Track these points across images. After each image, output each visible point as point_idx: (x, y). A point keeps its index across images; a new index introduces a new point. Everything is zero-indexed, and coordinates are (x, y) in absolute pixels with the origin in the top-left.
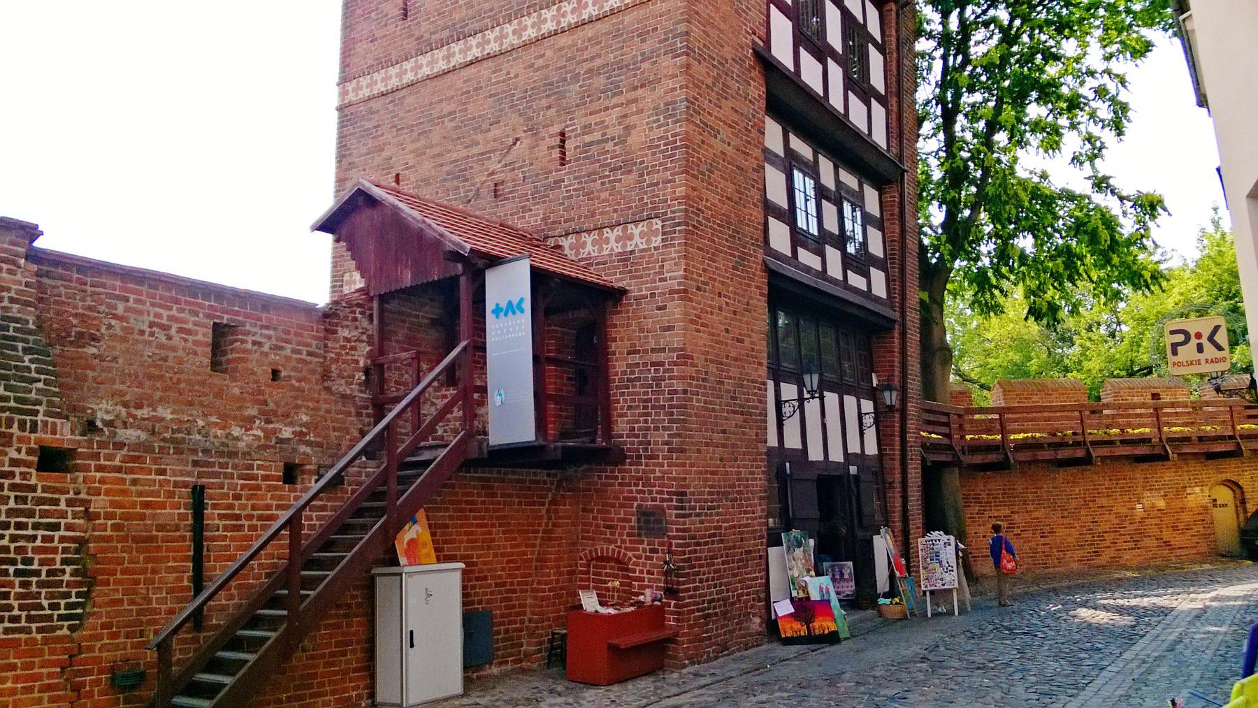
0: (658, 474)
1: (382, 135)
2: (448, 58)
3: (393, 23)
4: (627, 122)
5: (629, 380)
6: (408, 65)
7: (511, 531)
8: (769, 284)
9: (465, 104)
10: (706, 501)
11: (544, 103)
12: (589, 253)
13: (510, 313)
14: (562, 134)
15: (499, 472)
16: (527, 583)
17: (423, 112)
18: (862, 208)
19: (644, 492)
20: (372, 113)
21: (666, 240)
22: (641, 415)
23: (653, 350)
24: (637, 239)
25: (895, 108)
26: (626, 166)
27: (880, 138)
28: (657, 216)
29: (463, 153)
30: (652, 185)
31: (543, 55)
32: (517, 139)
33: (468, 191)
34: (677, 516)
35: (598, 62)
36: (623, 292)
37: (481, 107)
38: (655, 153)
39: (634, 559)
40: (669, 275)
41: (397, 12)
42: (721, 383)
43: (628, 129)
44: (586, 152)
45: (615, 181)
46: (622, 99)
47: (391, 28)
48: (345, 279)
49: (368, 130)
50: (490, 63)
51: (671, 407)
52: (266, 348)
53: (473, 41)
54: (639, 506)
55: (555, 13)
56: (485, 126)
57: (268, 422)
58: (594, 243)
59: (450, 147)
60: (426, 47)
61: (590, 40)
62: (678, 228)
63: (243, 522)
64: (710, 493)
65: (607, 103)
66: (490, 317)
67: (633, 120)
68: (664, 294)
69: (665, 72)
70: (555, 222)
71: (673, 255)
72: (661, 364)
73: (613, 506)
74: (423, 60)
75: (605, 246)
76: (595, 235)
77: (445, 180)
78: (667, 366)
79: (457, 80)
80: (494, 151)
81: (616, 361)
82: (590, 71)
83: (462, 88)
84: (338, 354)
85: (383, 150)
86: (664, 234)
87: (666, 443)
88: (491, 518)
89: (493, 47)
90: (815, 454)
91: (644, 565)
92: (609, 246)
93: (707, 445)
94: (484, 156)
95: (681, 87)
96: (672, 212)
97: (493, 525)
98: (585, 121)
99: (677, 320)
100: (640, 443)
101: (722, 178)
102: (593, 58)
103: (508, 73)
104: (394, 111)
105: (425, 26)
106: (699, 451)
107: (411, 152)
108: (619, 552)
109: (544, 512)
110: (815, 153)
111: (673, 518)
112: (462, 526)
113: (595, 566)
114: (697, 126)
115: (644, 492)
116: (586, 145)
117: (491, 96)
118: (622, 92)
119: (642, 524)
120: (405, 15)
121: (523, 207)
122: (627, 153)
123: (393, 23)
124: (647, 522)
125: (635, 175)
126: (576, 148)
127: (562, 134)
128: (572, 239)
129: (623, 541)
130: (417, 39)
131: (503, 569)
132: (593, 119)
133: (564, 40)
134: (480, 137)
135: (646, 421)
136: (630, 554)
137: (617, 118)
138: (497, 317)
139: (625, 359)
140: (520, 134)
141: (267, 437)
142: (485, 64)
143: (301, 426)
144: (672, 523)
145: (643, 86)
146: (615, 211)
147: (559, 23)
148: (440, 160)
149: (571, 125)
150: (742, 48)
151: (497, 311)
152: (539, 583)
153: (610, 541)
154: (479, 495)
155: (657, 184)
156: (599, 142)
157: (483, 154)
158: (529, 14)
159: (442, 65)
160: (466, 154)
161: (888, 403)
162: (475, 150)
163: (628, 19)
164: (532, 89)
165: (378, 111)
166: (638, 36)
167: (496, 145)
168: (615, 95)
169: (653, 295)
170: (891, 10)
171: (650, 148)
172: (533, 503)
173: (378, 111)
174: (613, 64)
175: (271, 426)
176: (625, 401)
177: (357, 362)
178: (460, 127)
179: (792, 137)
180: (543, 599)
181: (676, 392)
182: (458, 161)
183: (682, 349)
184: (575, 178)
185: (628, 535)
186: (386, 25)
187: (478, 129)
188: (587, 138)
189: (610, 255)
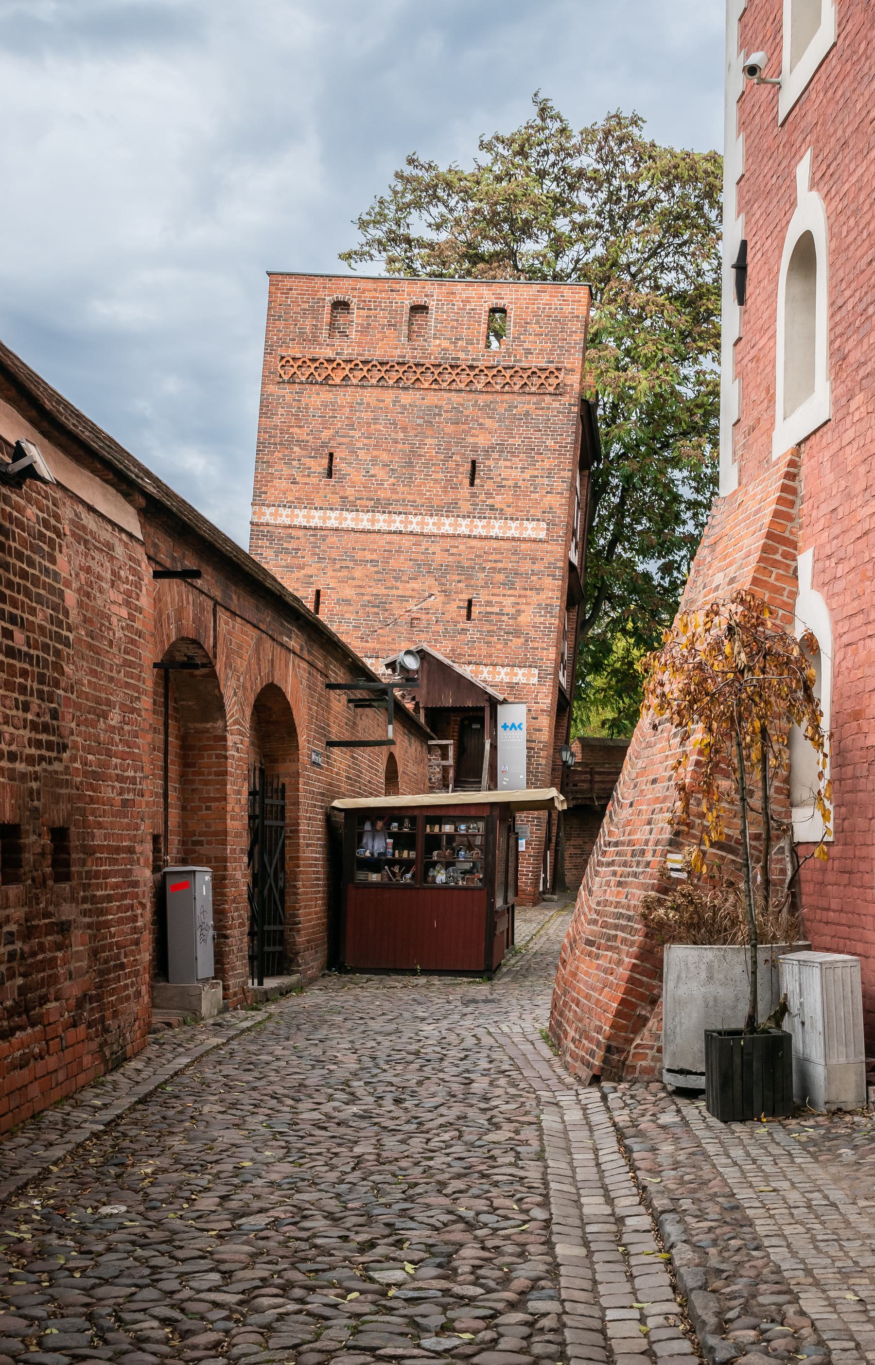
4: (519, 607)
11: (457, 578)
14: (470, 602)
26: (517, 633)
37: (398, 563)
46: (516, 593)
47: (314, 480)
56: (404, 578)
58: (489, 672)
60: (348, 506)
61: (494, 549)
65: (505, 592)
67: (523, 607)
72: (533, 749)
76: (490, 668)
79: (383, 541)
82: (494, 569)
94: (403, 598)
98: (487, 598)
102: (496, 561)
103: (427, 549)
116: (487, 613)
120: (330, 474)
125: (522, 640)
132: (495, 599)
142: (406, 537)
145: (531, 589)
147: (471, 531)
148: (362, 591)
156: (497, 614)
159: (367, 526)
163: (523, 546)
167: (414, 593)
168: (511, 588)
187: (397, 579)
188: (489, 609)
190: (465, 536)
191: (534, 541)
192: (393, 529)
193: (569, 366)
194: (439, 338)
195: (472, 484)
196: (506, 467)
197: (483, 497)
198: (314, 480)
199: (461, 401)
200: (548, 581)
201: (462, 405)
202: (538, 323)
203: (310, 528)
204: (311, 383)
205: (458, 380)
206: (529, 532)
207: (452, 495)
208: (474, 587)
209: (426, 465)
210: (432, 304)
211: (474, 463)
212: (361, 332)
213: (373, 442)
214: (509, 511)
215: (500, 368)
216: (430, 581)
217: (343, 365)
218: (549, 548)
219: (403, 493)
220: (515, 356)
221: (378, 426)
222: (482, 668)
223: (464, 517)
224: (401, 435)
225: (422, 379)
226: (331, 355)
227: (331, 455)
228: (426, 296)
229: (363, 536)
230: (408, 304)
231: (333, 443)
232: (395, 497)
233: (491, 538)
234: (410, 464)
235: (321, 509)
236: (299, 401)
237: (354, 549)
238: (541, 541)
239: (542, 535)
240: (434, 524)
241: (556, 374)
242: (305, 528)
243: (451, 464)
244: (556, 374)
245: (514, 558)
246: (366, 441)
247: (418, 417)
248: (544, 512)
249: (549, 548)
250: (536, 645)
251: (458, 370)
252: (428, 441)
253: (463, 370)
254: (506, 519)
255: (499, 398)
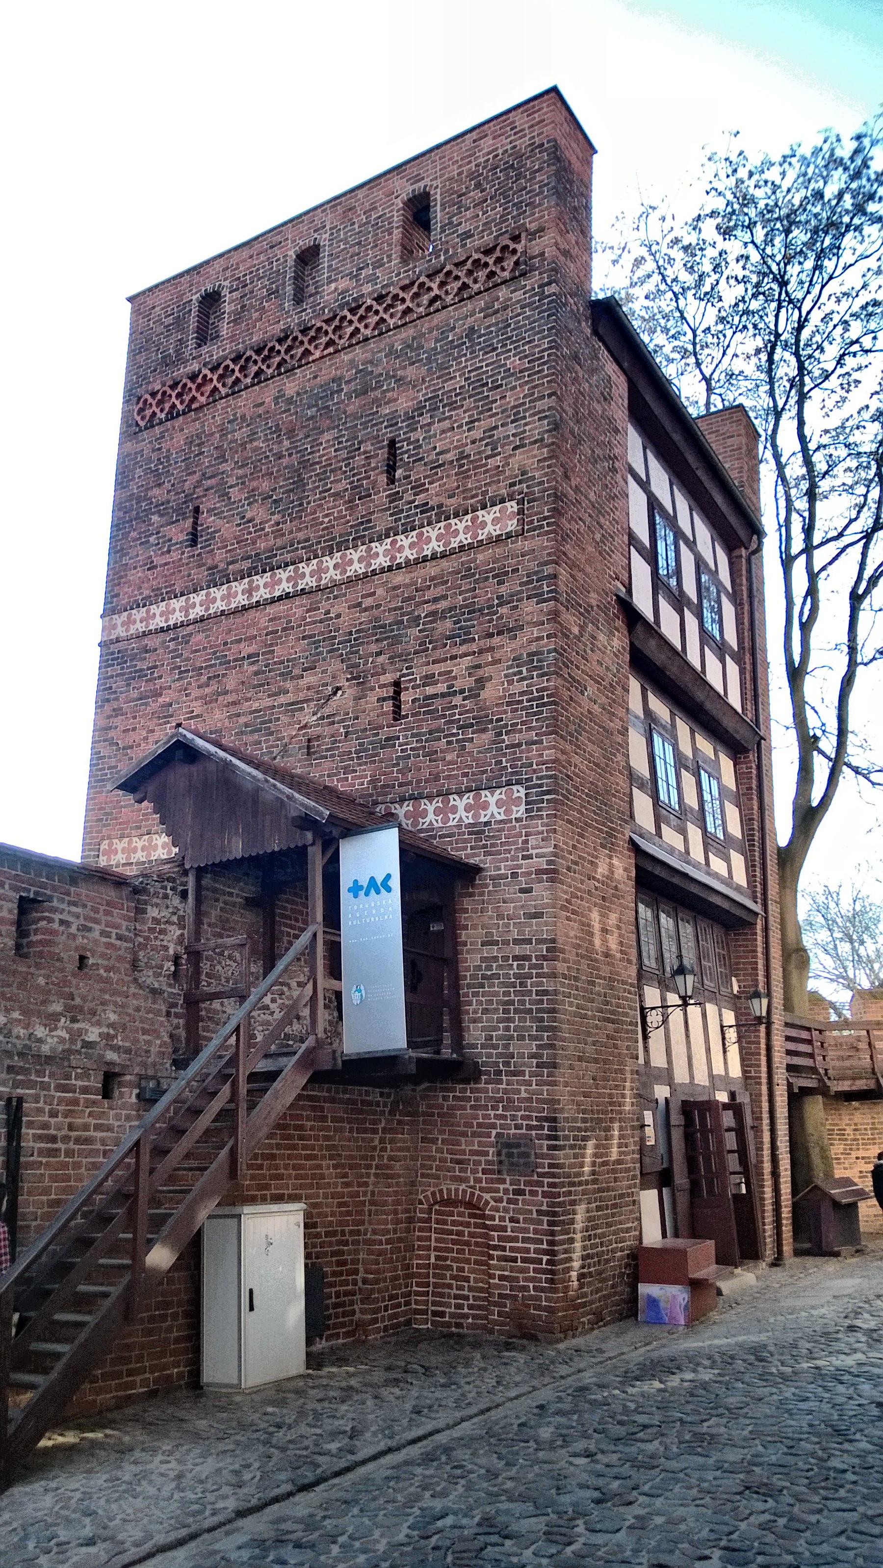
0: (524, 1095)
1: (160, 677)
2: (249, 592)
3: (177, 549)
4: (480, 672)
5: (484, 977)
6: (197, 598)
7: (343, 1166)
8: (637, 867)
9: (271, 645)
10: (579, 1129)
11: (374, 648)
12: (431, 823)
13: (373, 891)
15: (329, 1091)
16: (358, 1233)
17: (215, 653)
18: (719, 779)
19: (504, 1117)
20: (147, 652)
21: (532, 810)
22: (500, 1021)
23: (516, 942)
24: (493, 808)
25: (748, 667)
26: (480, 723)
27: (735, 699)
28: (518, 782)
29: (268, 702)
30: (513, 746)
31: (374, 594)
32: (338, 689)
33: (272, 746)
34: (550, 1148)
35: (443, 605)
36: (477, 870)
38: (516, 710)
39: (492, 1203)
40: (534, 852)
41: (183, 537)
42: (593, 983)
43: (481, 682)
44: (428, 705)
45: (464, 740)
46: (474, 647)
47: (175, 555)
48: (102, 847)
49: (141, 670)
50: (304, 600)
51: (539, 1010)
52: (73, 929)
53: (283, 575)
54: (498, 1135)
55: (389, 547)
56: (297, 671)
57: (74, 1020)
58: (437, 812)
59: (249, 695)
61: (432, 579)
62: (546, 797)
63: (59, 1145)
64: (584, 1120)
65: (455, 651)
66: (345, 897)
67: (487, 671)
68: (529, 874)
69: (529, 618)
70: (388, 786)
71: (540, 828)
72: (527, 958)
73: (464, 1134)
74: (217, 593)
75: (451, 816)
76: (438, 803)
77: (242, 733)
78: (534, 961)
79: (262, 618)
80: (306, 701)
81: (468, 952)
82: (433, 613)
83: (267, 627)
84: (147, 939)
85: (161, 695)
86: (527, 803)
87: (532, 1056)
88: (321, 1148)
89: (309, 582)
90: (681, 1075)
91: (506, 1210)
92: (457, 816)
93: (580, 1059)
94: (294, 707)
95: (548, 637)
96: (538, 778)
97: (323, 1157)
98: (425, 670)
99: (547, 906)
100: (499, 1055)
101: (590, 740)
102: (436, 600)
103: (328, 612)
104: (176, 650)
105: (220, 555)
106: (571, 1067)
107: (196, 699)
108: (472, 1194)
109: (376, 1142)
110: (672, 714)
111: (545, 1151)
112: (290, 1157)
113: (438, 1212)
114: (565, 679)
115: (504, 1117)
117: (304, 638)
118: (474, 639)
119: (503, 1158)
121: (345, 768)
122: (481, 709)
123: (177, 549)
124: (510, 1155)
126: (413, 701)
127: (397, 684)
128: (407, 807)
129: (480, 1181)
130: (209, 569)
131: (333, 1214)
132: (437, 669)
133: (399, 578)
134: (289, 685)
135: (507, 1029)
136: (487, 1196)
137: (467, 668)
138: (356, 896)
139: (480, 951)
140: (343, 683)
141: (72, 1041)
142: (298, 601)
143: (109, 1026)
144: (543, 1156)
146: (465, 775)
149: (408, 675)
150: (607, 594)
151: (356, 889)
152: (374, 1232)
153: (461, 1180)
154: (308, 1119)
155: (519, 745)
156: (443, 695)
157: (292, 704)
158: (355, 547)
160: (270, 704)
161: (758, 1014)
162: (282, 699)
163: (480, 557)
164: (358, 632)
165: (156, 650)
166: (494, 577)
168: (464, 642)
169: (514, 875)
170: (741, 556)
171: (509, 704)
172: (365, 1131)
173: (156, 650)
174: (462, 607)
175: (76, 1026)
176: (480, 1003)
177: (166, 948)
178: (264, 672)
179: (651, 697)
180: (380, 1253)
181: (545, 993)
182: (260, 711)
183: (554, 941)
184: (413, 736)
185: (484, 1172)
186: (169, 551)
188: (430, 691)
189: (459, 826)
190: (382, 570)
191: (499, 540)
192: (277, 594)
193: (533, 227)
194: (336, 280)
195: (392, 481)
196: (443, 432)
197: (409, 497)
198: (175, 555)
199: (369, 355)
200: (530, 608)
201: (371, 362)
202: (478, 185)
203: (169, 628)
204: (173, 418)
205: (361, 326)
206: (490, 528)
207: (361, 510)
208: (404, 657)
209: (322, 477)
210: (324, 239)
211: (392, 443)
212: (235, 320)
213: (247, 471)
214: (452, 503)
215: (423, 279)
216: (335, 665)
217: (209, 376)
218: (527, 545)
219: (291, 532)
220: (447, 251)
221: (255, 444)
222: (425, 804)
223: (380, 539)
224: (286, 443)
225: (311, 348)
226: (195, 366)
227: (197, 510)
228: (315, 231)
229: (238, 620)
230: (292, 254)
231: (199, 491)
232: (279, 543)
233: (425, 559)
234: (300, 484)
235: (182, 595)
236: (160, 449)
237: (226, 644)
238: (509, 536)
239: (512, 525)
240: (336, 567)
241: (512, 246)
242: (162, 630)
243: (359, 460)
244: (512, 246)
245: (465, 585)
246: (240, 472)
247: (309, 408)
248: (512, 485)
249: (527, 545)
250: (517, 738)
251: (361, 311)
252: (327, 436)
253: (369, 308)
254: (448, 518)
255: (425, 325)
